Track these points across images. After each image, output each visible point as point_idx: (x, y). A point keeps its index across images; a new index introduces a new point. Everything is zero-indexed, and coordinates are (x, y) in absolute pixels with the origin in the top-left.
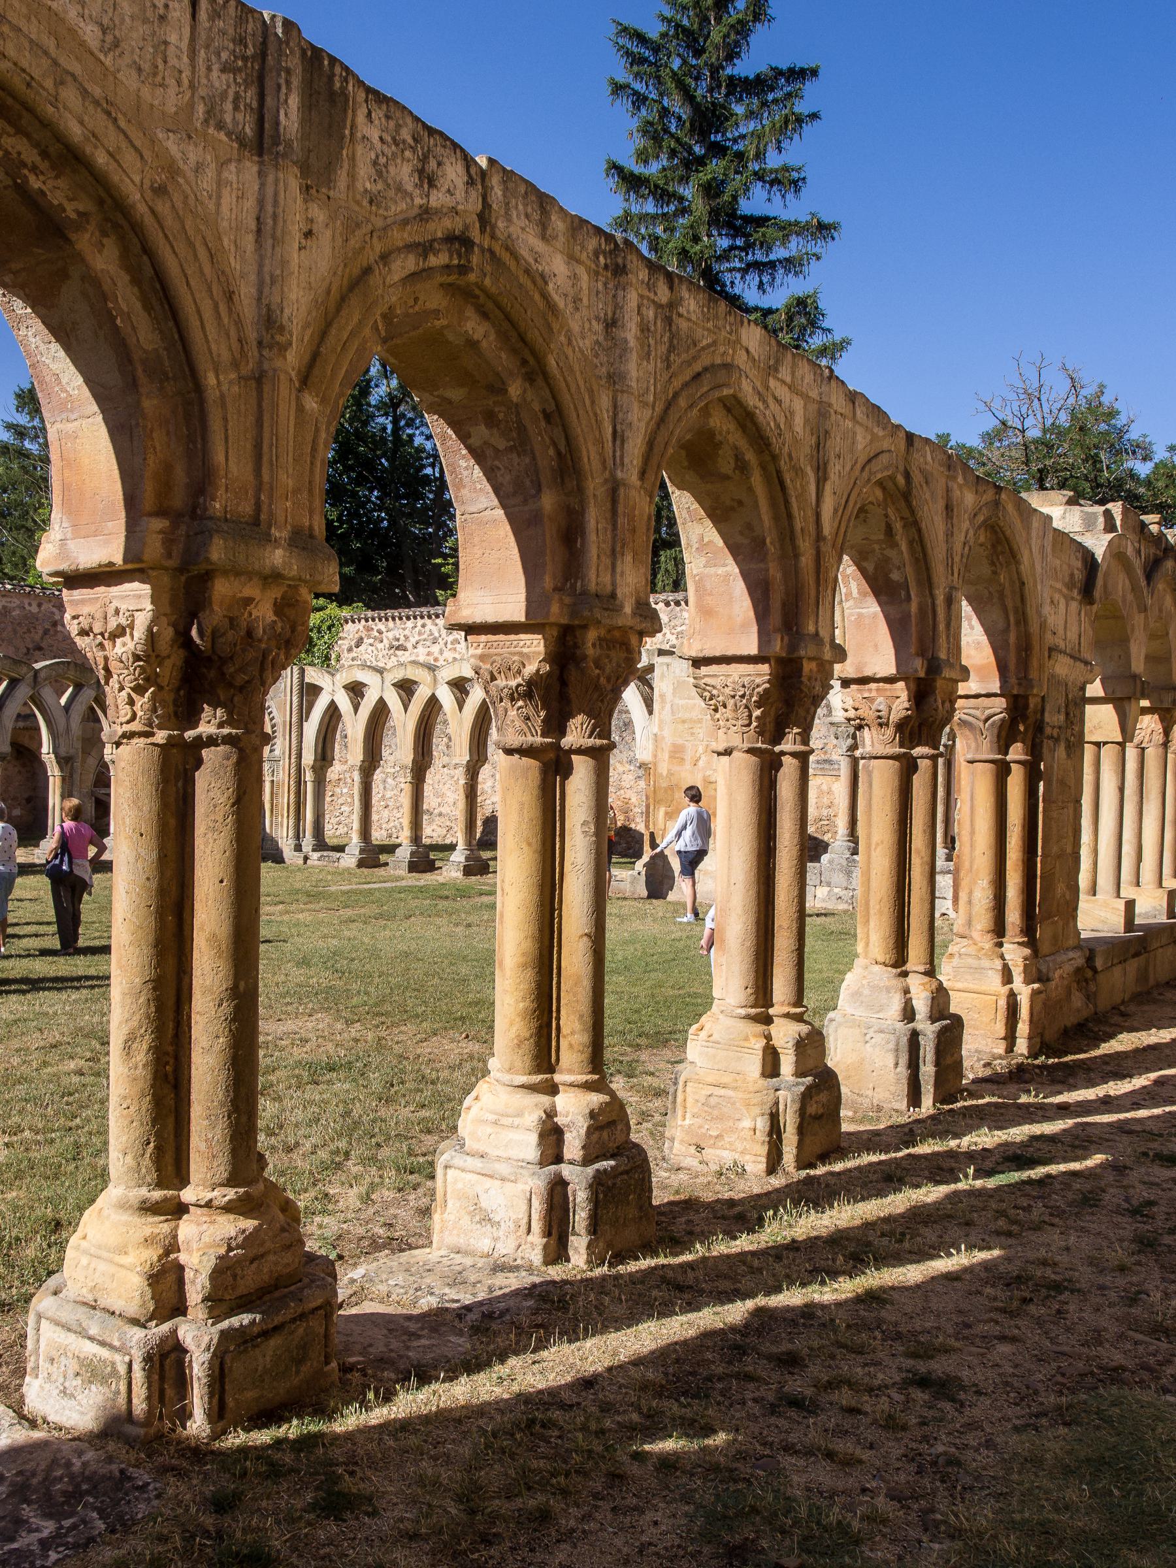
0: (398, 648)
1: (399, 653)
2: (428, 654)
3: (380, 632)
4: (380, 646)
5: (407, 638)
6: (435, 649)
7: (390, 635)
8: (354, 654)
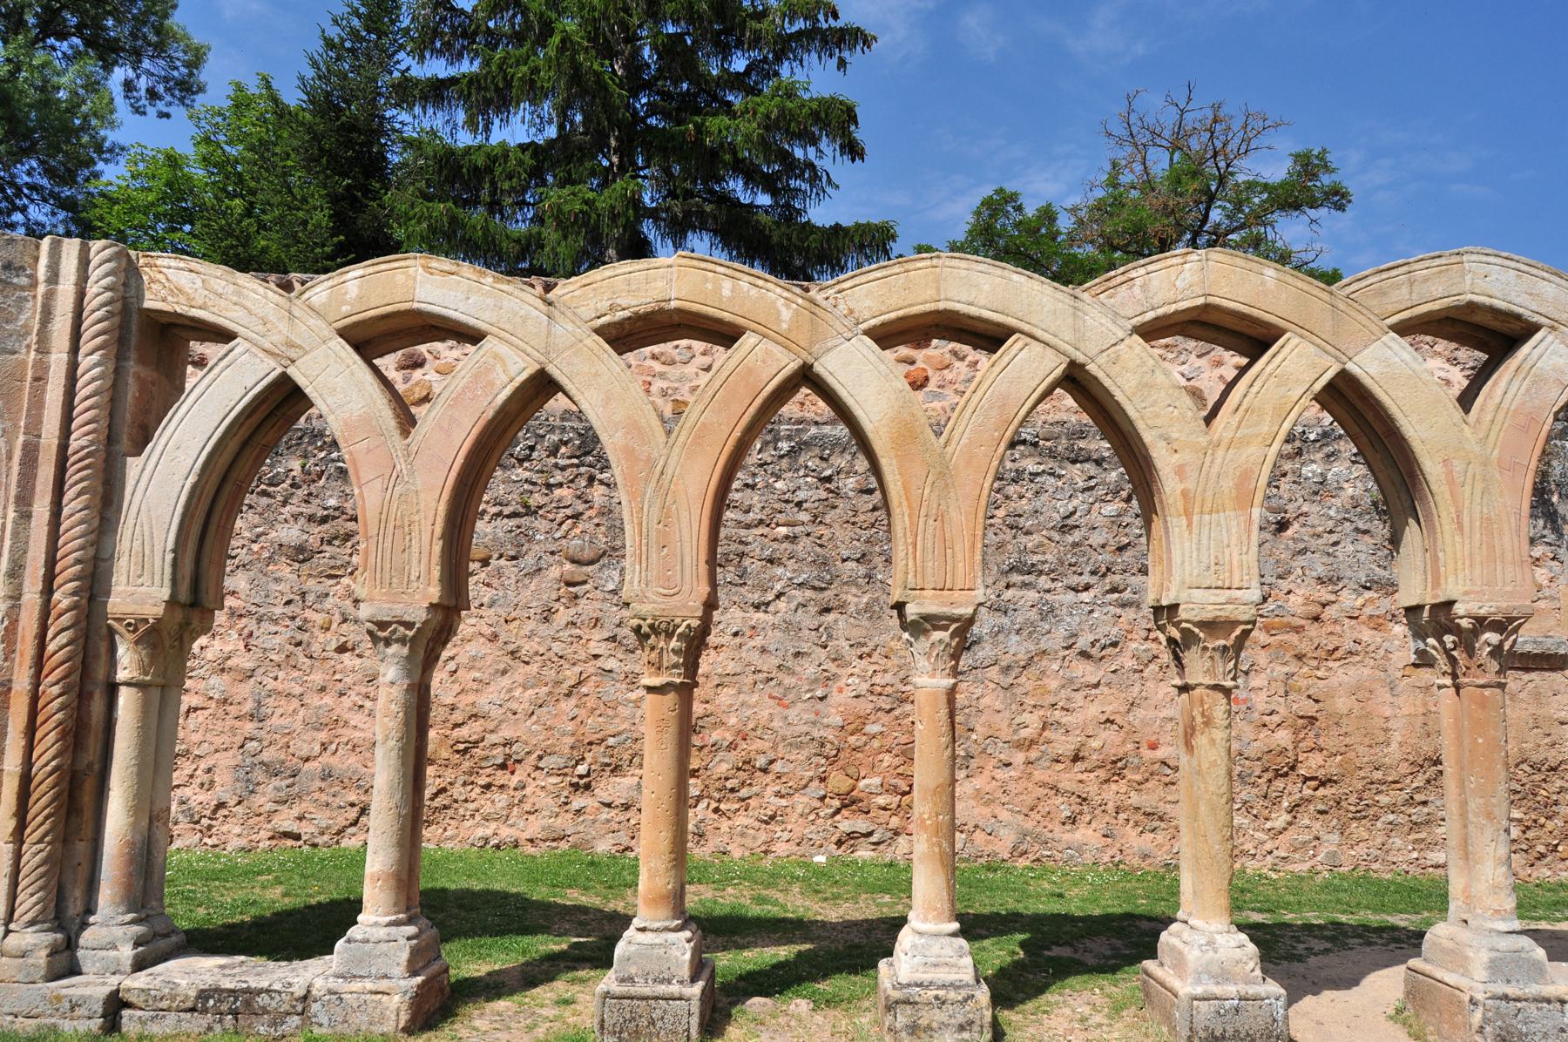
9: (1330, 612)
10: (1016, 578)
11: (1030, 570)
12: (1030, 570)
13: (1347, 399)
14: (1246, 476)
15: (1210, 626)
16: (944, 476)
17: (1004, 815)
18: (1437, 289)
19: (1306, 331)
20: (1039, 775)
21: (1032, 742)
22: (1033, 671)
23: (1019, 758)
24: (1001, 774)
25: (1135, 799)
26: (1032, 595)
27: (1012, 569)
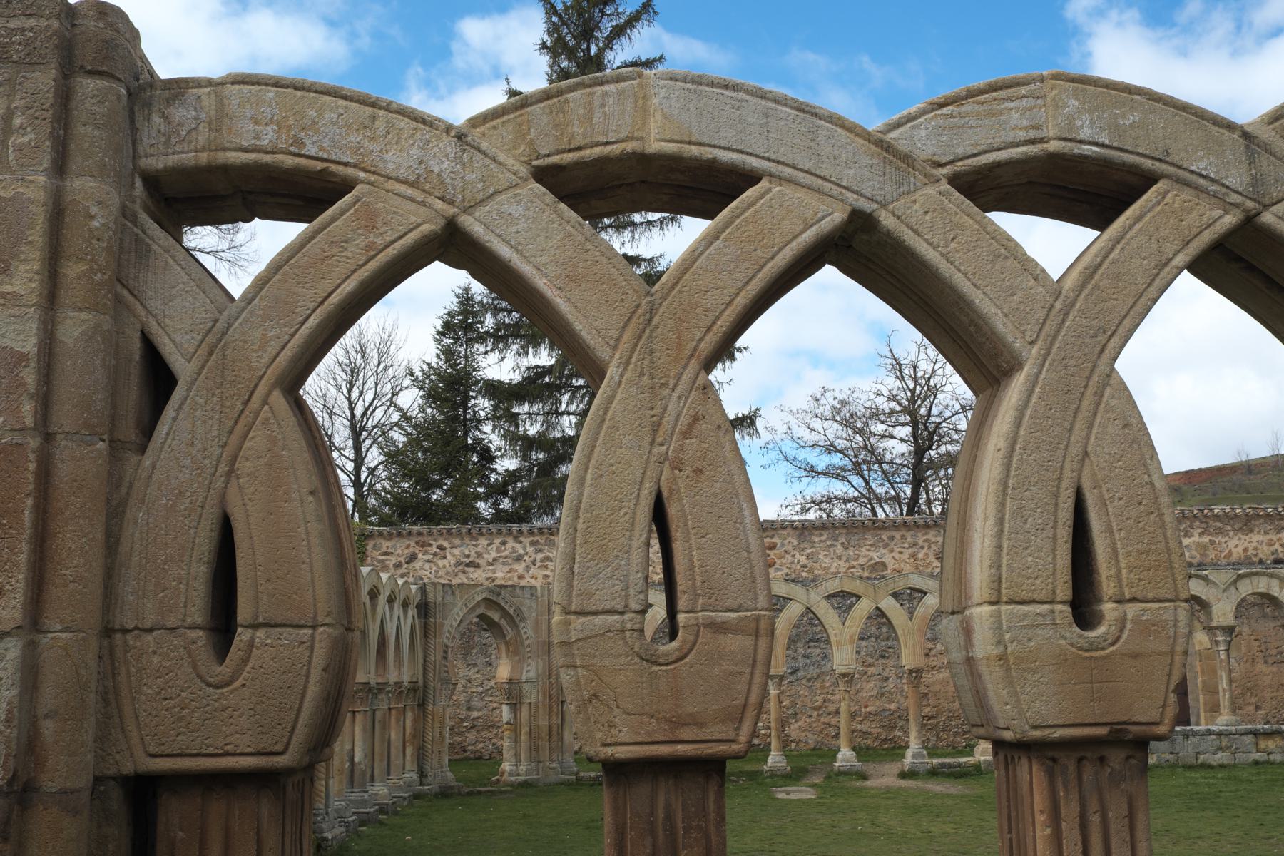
0: (467, 565)
1: (471, 569)
2: (510, 571)
3: (441, 548)
4: (441, 563)
5: (479, 555)
6: (520, 567)
7: (456, 551)
8: (403, 570)
9: (933, 652)
11: (818, 641)
12: (818, 641)
13: (880, 613)
15: (844, 675)
17: (810, 735)
20: (823, 720)
25: (859, 727)
26: (818, 651)
27: (811, 641)
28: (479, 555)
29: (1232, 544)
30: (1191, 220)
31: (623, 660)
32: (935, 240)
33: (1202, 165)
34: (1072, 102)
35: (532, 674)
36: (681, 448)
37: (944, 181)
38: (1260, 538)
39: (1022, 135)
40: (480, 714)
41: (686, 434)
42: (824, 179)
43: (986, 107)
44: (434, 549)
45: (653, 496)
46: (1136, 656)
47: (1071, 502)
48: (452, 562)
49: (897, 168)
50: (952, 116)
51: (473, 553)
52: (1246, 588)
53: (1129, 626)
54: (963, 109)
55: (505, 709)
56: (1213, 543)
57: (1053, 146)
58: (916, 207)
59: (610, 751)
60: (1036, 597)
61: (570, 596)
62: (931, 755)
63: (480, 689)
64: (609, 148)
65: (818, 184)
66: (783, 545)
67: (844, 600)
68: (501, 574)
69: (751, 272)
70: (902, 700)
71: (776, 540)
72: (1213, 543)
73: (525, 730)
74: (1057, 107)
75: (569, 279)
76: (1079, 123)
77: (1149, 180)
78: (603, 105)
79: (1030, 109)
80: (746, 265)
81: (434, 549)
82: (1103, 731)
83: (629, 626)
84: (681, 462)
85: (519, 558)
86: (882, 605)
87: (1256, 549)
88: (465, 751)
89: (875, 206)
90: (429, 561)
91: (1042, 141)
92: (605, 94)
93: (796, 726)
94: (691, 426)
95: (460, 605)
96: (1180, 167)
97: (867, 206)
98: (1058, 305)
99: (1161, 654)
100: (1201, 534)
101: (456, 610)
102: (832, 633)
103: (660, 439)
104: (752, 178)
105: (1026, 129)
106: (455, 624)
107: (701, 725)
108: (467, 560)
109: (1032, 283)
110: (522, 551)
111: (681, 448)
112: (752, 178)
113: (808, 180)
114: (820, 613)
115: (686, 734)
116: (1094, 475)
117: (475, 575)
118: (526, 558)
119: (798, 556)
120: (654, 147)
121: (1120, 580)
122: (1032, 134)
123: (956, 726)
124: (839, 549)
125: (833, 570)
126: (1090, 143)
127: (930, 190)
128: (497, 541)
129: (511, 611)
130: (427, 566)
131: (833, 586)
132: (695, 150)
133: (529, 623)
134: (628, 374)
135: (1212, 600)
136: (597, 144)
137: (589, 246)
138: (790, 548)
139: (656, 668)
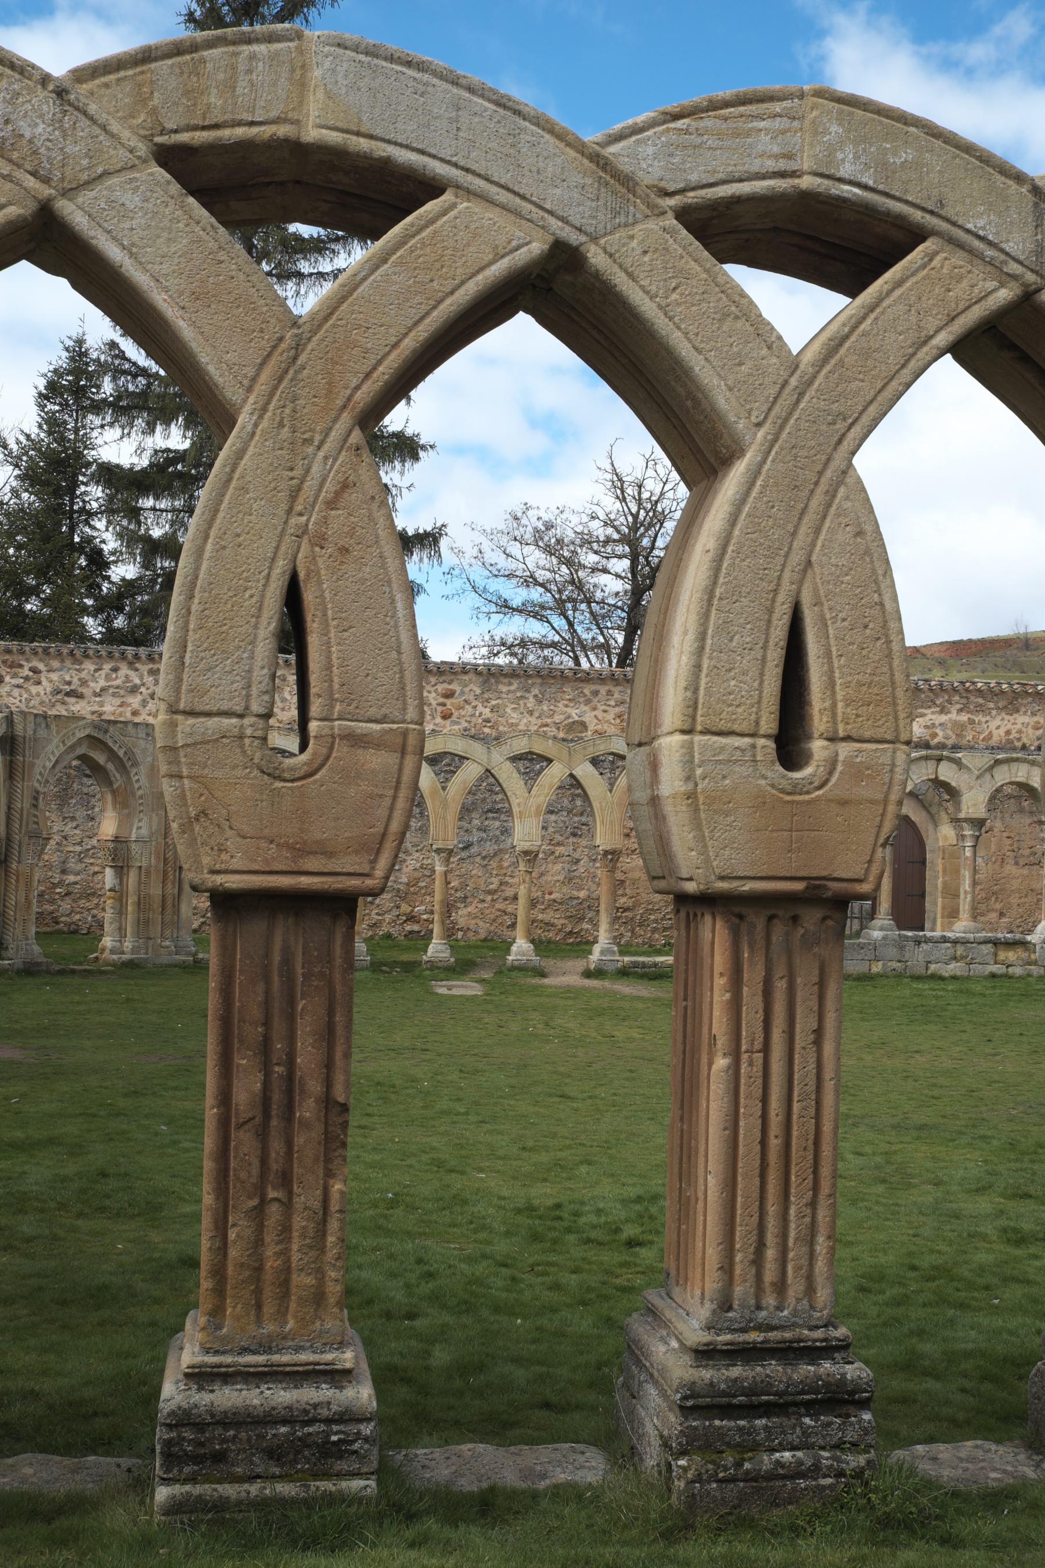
0: (68, 694)
1: (72, 700)
3: (35, 671)
4: (34, 690)
5: (83, 683)
6: (135, 701)
7: (54, 676)
10: (490, 815)
11: (498, 811)
12: (498, 811)
13: (575, 782)
14: (538, 807)
15: (526, 853)
16: (445, 804)
17: (481, 924)
18: (602, 747)
19: (560, 760)
20: (497, 906)
21: (496, 891)
22: (497, 859)
23: (489, 898)
24: (480, 906)
25: (540, 917)
26: (497, 824)
27: (489, 811)
28: (83, 683)
29: (993, 725)
30: (960, 291)
31: (239, 772)
32: (654, 288)
33: (981, 223)
34: (834, 128)
35: (144, 832)
36: (325, 521)
37: (670, 215)
38: (1026, 719)
39: (770, 165)
40: (78, 878)
41: (332, 504)
42: (523, 197)
43: (731, 124)
44: (26, 672)
45: (287, 577)
46: (844, 803)
47: (786, 620)
48: (49, 690)
49: (614, 193)
50: (687, 132)
51: (75, 680)
52: (1003, 776)
53: (840, 768)
54: (702, 124)
55: (109, 872)
56: (971, 722)
57: (806, 182)
58: (634, 244)
59: (219, 879)
60: (736, 727)
61: (178, 691)
62: (622, 953)
63: (78, 848)
64: (255, 130)
65: (516, 201)
66: (462, 693)
67: (531, 763)
68: (110, 708)
69: (424, 308)
70: (594, 887)
71: (455, 687)
72: (971, 722)
73: (132, 900)
74: (816, 133)
75: (196, 296)
76: (840, 156)
77: (916, 236)
78: (250, 71)
79: (783, 132)
80: (418, 299)
81: (26, 672)
82: (798, 886)
83: (249, 732)
84: (323, 537)
85: (134, 690)
86: (578, 772)
87: (1020, 732)
88: (57, 923)
89: (583, 238)
90: (18, 686)
91: (794, 174)
92: (253, 57)
93: (465, 911)
94: (338, 494)
95: (56, 741)
96: (954, 224)
97: (574, 238)
98: (793, 381)
99: (872, 802)
100: (961, 710)
101: (50, 748)
102: (514, 802)
103: (299, 508)
104: (433, 188)
105: (776, 157)
106: (49, 765)
107: (330, 855)
108: (67, 688)
109: (765, 351)
110: (137, 681)
111: (325, 521)
112: (433, 188)
113: (503, 197)
114: (502, 777)
115: (312, 864)
116: (816, 590)
117: (78, 707)
118: (143, 689)
119: (480, 708)
120: (312, 134)
121: (834, 715)
122: (782, 165)
123: (656, 921)
124: (531, 703)
125: (521, 727)
126: (851, 183)
127: (652, 225)
128: (107, 667)
129: (121, 753)
130: (16, 692)
131: (520, 745)
132: (364, 145)
133: (143, 770)
134: (264, 424)
135: (963, 789)
136: (240, 124)
137: (222, 256)
138: (472, 698)
139: (279, 784)
